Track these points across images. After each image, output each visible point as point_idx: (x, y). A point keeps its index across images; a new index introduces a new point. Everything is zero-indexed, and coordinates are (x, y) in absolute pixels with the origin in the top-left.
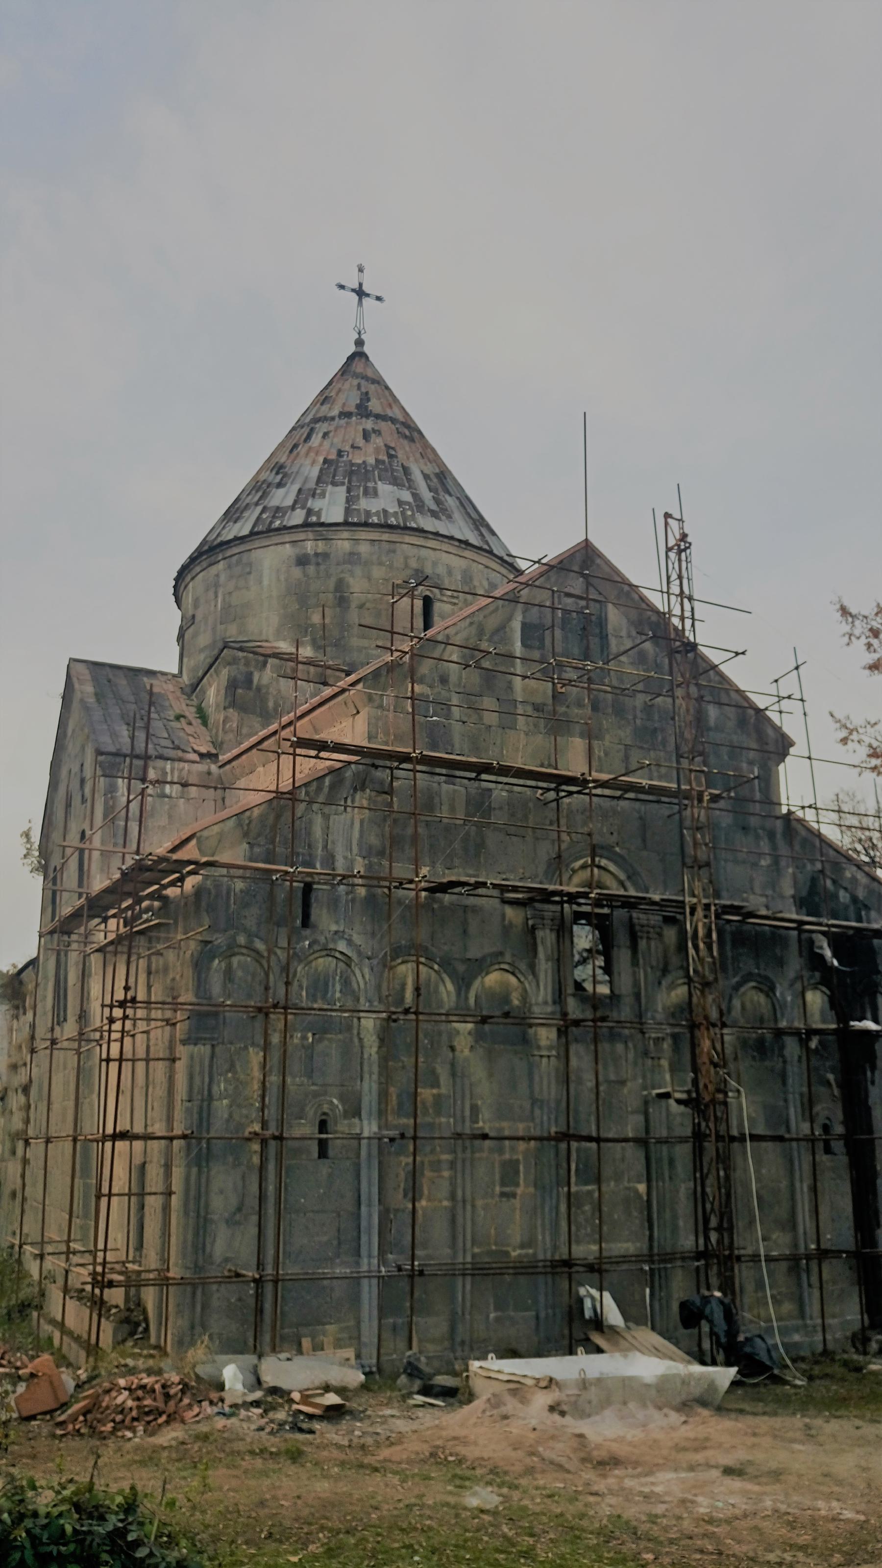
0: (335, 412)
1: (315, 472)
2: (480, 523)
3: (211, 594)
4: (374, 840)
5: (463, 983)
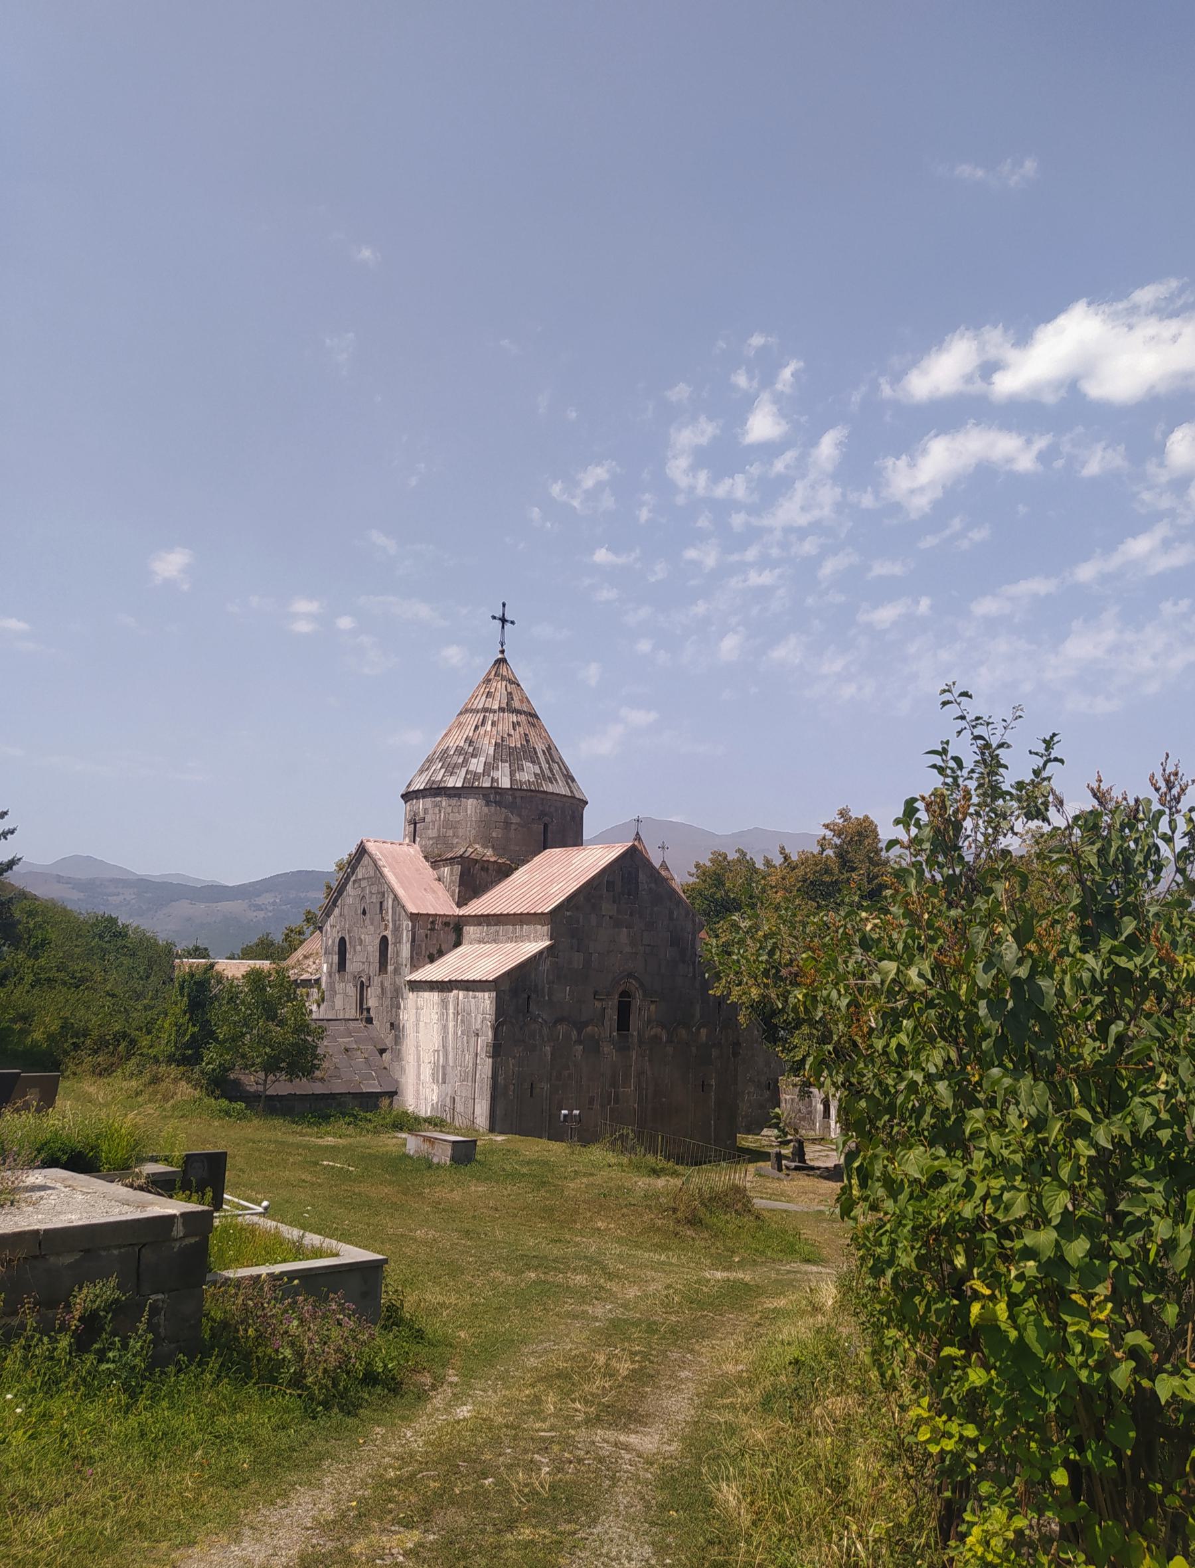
0: (496, 707)
1: (491, 751)
2: (569, 778)
3: (437, 810)
4: (551, 977)
5: (579, 1033)
